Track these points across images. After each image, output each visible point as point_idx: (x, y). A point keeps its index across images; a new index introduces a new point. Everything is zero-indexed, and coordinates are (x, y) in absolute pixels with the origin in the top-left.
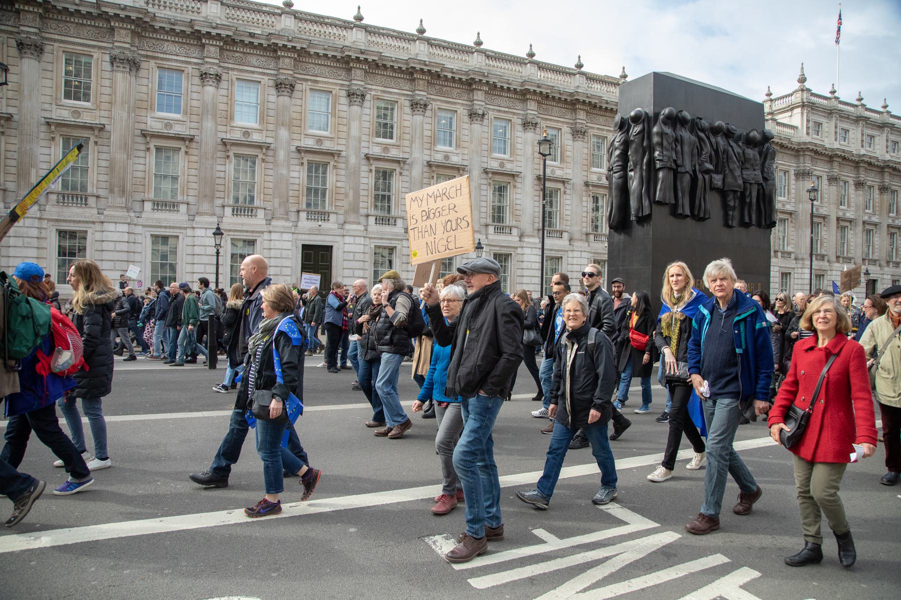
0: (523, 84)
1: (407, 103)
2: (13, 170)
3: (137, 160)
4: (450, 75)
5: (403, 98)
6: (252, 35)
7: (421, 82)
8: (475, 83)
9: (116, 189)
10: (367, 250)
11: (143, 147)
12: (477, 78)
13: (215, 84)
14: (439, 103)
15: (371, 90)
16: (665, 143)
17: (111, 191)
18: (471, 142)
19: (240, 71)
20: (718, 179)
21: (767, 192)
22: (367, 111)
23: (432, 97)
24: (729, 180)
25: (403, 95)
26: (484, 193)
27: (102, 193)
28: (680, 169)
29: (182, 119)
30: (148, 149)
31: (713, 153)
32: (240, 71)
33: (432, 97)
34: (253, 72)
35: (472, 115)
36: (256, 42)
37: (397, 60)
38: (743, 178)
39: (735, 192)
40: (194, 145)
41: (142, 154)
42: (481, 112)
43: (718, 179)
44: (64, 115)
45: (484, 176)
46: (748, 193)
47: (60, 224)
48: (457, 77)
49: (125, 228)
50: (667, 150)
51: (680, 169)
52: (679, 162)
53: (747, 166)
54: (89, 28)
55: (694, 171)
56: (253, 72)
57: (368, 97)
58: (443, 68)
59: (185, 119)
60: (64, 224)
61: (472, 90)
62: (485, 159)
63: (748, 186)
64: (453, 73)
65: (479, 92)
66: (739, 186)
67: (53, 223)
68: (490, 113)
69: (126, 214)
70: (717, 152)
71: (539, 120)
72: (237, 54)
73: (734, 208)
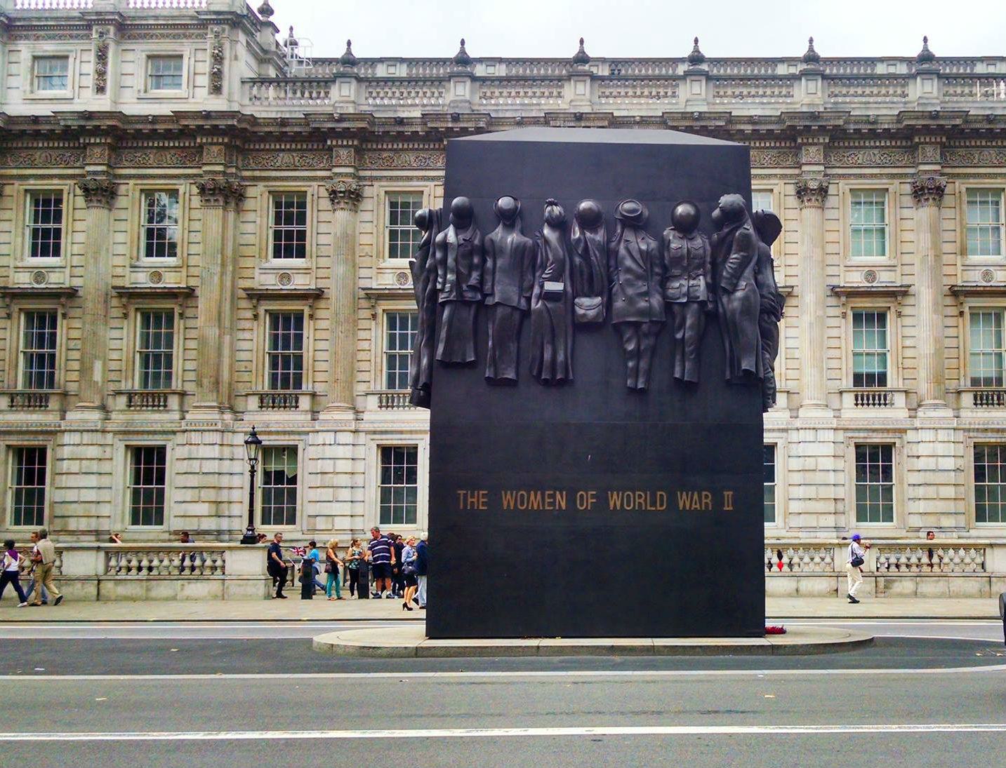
0: (900, 117)
2: (76, 365)
3: (241, 335)
4: (748, 128)
6: (400, 121)
8: (800, 133)
9: (205, 381)
11: (249, 314)
12: (800, 124)
13: (350, 206)
16: (450, 261)
17: (199, 384)
18: (803, 243)
19: (391, 178)
20: (588, 306)
21: (729, 314)
24: (619, 304)
26: (835, 332)
27: (190, 387)
28: (489, 301)
29: (305, 266)
30: (256, 317)
31: (577, 260)
32: (391, 178)
34: (409, 178)
35: (802, 192)
36: (408, 130)
38: (664, 296)
39: (636, 325)
40: (322, 304)
41: (247, 325)
42: (813, 185)
43: (588, 306)
44: (142, 280)
45: (833, 301)
46: (677, 321)
48: (763, 128)
49: (216, 437)
50: (452, 271)
51: (489, 301)
52: (488, 287)
55: (529, 300)
56: (409, 178)
59: (309, 265)
61: (799, 147)
62: (831, 271)
63: (676, 308)
64: (754, 123)
65: (813, 149)
66: (641, 312)
68: (842, 182)
69: (217, 417)
71: (943, 181)
72: (385, 155)
73: (637, 354)
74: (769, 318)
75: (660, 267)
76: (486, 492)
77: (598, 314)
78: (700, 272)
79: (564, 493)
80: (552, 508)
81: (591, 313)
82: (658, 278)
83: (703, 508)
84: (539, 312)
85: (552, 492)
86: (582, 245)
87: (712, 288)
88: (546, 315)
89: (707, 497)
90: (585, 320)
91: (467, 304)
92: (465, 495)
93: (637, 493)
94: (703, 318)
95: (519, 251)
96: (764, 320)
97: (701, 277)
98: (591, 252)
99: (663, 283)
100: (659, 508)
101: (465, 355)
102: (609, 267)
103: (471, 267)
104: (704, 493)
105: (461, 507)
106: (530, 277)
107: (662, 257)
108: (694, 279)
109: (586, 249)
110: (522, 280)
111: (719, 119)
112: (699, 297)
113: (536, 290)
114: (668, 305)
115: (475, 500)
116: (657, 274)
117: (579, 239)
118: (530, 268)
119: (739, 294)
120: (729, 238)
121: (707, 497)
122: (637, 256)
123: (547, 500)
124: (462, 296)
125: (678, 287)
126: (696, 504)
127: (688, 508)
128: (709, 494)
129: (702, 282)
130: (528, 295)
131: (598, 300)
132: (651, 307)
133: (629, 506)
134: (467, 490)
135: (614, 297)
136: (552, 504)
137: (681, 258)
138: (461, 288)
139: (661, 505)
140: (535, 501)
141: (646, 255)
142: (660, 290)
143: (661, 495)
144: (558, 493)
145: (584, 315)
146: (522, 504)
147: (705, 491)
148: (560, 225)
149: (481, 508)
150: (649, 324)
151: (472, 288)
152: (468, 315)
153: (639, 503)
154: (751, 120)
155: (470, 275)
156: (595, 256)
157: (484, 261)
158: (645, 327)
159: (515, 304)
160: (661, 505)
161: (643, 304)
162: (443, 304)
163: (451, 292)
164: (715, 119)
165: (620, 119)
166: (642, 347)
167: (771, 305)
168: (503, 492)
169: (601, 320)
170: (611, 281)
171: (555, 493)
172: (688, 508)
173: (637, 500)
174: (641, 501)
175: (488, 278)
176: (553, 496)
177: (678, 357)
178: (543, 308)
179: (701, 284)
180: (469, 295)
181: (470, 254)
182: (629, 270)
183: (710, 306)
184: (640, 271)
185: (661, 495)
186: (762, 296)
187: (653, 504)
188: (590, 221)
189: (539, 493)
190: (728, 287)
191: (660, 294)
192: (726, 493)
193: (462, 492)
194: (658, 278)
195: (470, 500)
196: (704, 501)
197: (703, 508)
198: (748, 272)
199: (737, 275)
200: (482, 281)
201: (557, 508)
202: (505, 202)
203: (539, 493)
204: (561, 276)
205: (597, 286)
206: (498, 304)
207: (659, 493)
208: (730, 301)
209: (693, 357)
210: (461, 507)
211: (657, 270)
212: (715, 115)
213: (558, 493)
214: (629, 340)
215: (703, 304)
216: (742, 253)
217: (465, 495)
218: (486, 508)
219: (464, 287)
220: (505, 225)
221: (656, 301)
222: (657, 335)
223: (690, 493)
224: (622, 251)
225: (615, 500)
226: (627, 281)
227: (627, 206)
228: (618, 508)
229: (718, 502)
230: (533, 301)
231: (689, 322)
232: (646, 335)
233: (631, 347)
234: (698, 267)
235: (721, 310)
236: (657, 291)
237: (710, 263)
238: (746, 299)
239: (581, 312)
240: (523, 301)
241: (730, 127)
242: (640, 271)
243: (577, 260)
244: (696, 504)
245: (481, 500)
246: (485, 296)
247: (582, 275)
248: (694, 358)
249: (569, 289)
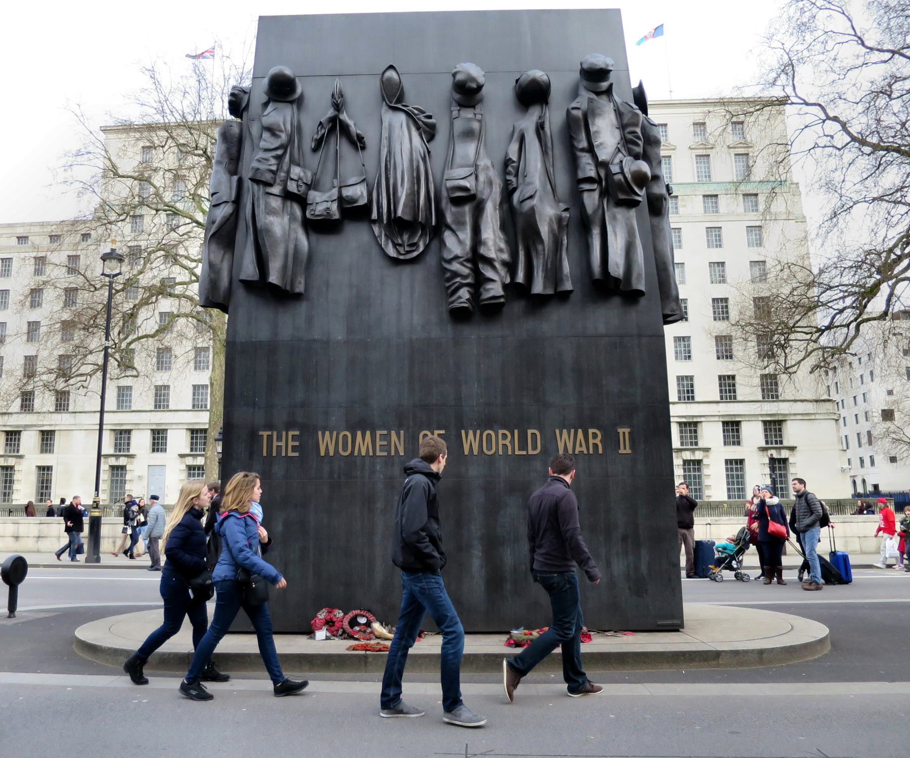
76: (297, 433)
79: (402, 432)
80: (385, 454)
83: (591, 452)
85: (385, 432)
89: (595, 436)
92: (270, 438)
93: (501, 432)
100: (531, 452)
104: (591, 431)
105: (265, 454)
115: (283, 444)
121: (595, 436)
123: (378, 443)
126: (581, 445)
127: (570, 452)
133: (489, 449)
136: (387, 448)
139: (535, 448)
140: (363, 444)
143: (534, 434)
144: (393, 433)
146: (345, 448)
147: (593, 428)
149: (290, 454)
153: (505, 446)
160: (535, 448)
168: (320, 433)
171: (389, 434)
172: (570, 452)
173: (501, 442)
176: (387, 438)
185: (534, 434)
187: (523, 446)
189: (368, 433)
192: (621, 431)
193: (265, 434)
195: (275, 444)
196: (591, 441)
197: (591, 452)
201: (393, 454)
203: (368, 433)
210: (265, 454)
213: (393, 433)
217: (270, 438)
218: (296, 454)
223: (572, 431)
225: (470, 441)
228: (475, 453)
229: (611, 440)
244: (581, 445)
245: (291, 444)
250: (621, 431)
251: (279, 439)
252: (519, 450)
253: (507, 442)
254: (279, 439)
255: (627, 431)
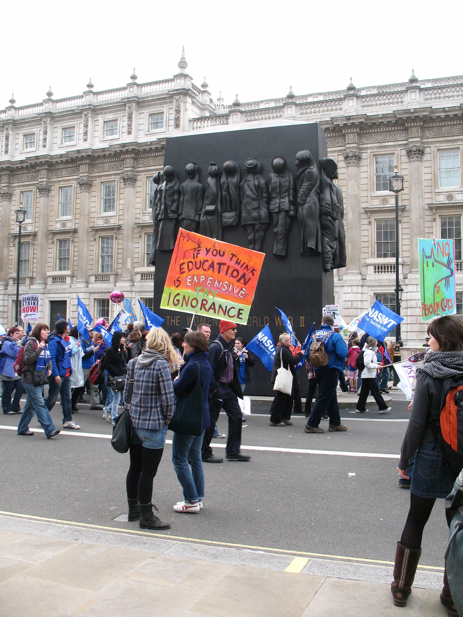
1: (404, 152)
4: (443, 115)
5: (399, 149)
7: (414, 130)
10: (365, 297)
14: (438, 145)
15: (367, 148)
20: (229, 217)
21: (301, 217)
22: (364, 169)
23: (430, 140)
24: (244, 215)
25: (400, 145)
28: (180, 218)
31: (224, 193)
33: (430, 140)
37: (384, 116)
38: (268, 209)
39: (253, 225)
47: (142, 294)
48: (451, 114)
51: (180, 218)
53: (274, 195)
54: (159, 158)
55: (200, 215)
57: (364, 156)
58: (431, 110)
60: (144, 294)
63: (274, 215)
64: (446, 112)
66: (254, 219)
67: (138, 294)
70: (228, 190)
74: (326, 218)
75: (266, 194)
77: (233, 221)
78: (286, 194)
81: (230, 221)
82: (265, 199)
84: (204, 221)
86: (226, 185)
87: (294, 203)
88: (207, 222)
90: (226, 225)
91: (171, 219)
93: (254, 317)
94: (288, 220)
95: (195, 191)
96: (324, 220)
97: (287, 197)
98: (230, 188)
99: (268, 203)
101: (169, 246)
102: (240, 196)
103: (173, 201)
106: (200, 204)
107: (268, 188)
108: (283, 198)
109: (228, 187)
110: (197, 206)
111: (425, 111)
112: (284, 209)
113: (203, 211)
114: (270, 214)
115: (174, 321)
116: (265, 197)
117: (224, 182)
118: (201, 199)
119: (306, 206)
120: (303, 175)
122: (253, 189)
124: (168, 216)
125: (275, 204)
128: (292, 318)
129: (286, 200)
130: (199, 213)
131: (233, 214)
132: (259, 215)
134: (171, 316)
135: (242, 211)
137: (276, 188)
138: (167, 212)
141: (258, 188)
142: (266, 206)
145: (226, 222)
148: (216, 175)
149: (177, 325)
150: (259, 225)
151: (173, 211)
152: (171, 225)
154: (444, 110)
155: (172, 205)
156: (232, 190)
157: (180, 197)
158: (257, 227)
159: (192, 219)
161: (255, 214)
162: (160, 220)
163: (162, 214)
164: (423, 111)
165: (371, 117)
166: (256, 237)
167: (327, 210)
169: (235, 224)
170: (241, 203)
174: (256, 322)
175: (181, 206)
177: (275, 242)
178: (206, 219)
179: (285, 202)
180: (171, 215)
181: (173, 194)
182: (248, 196)
183: (292, 213)
184: (254, 196)
186: (321, 206)
188: (230, 172)
190: (301, 202)
191: (266, 208)
193: (168, 317)
194: (265, 199)
195: (172, 321)
198: (313, 193)
199: (307, 194)
200: (178, 208)
202: (189, 166)
204: (216, 202)
205: (233, 207)
206: (183, 219)
207: (265, 317)
208: (302, 210)
209: (282, 241)
211: (264, 195)
212: (423, 109)
214: (249, 234)
215: (287, 212)
216: (308, 182)
219: (169, 211)
220: (190, 178)
221: (263, 212)
222: (266, 230)
224: (246, 187)
226: (247, 202)
227: (250, 162)
230: (202, 216)
231: (280, 222)
232: (258, 231)
233: (250, 237)
234: (285, 192)
235: (298, 215)
236: (264, 207)
237: (292, 189)
238: (310, 207)
239: (226, 220)
240: (197, 217)
241: (432, 115)
242: (254, 196)
243: (224, 193)
245: (177, 321)
246: (179, 215)
247: (226, 200)
248: (282, 243)
249: (219, 208)
250: (301, 317)
251: (173, 319)
252: (261, 324)
253: (256, 322)
254: (173, 319)
255: (303, 317)
